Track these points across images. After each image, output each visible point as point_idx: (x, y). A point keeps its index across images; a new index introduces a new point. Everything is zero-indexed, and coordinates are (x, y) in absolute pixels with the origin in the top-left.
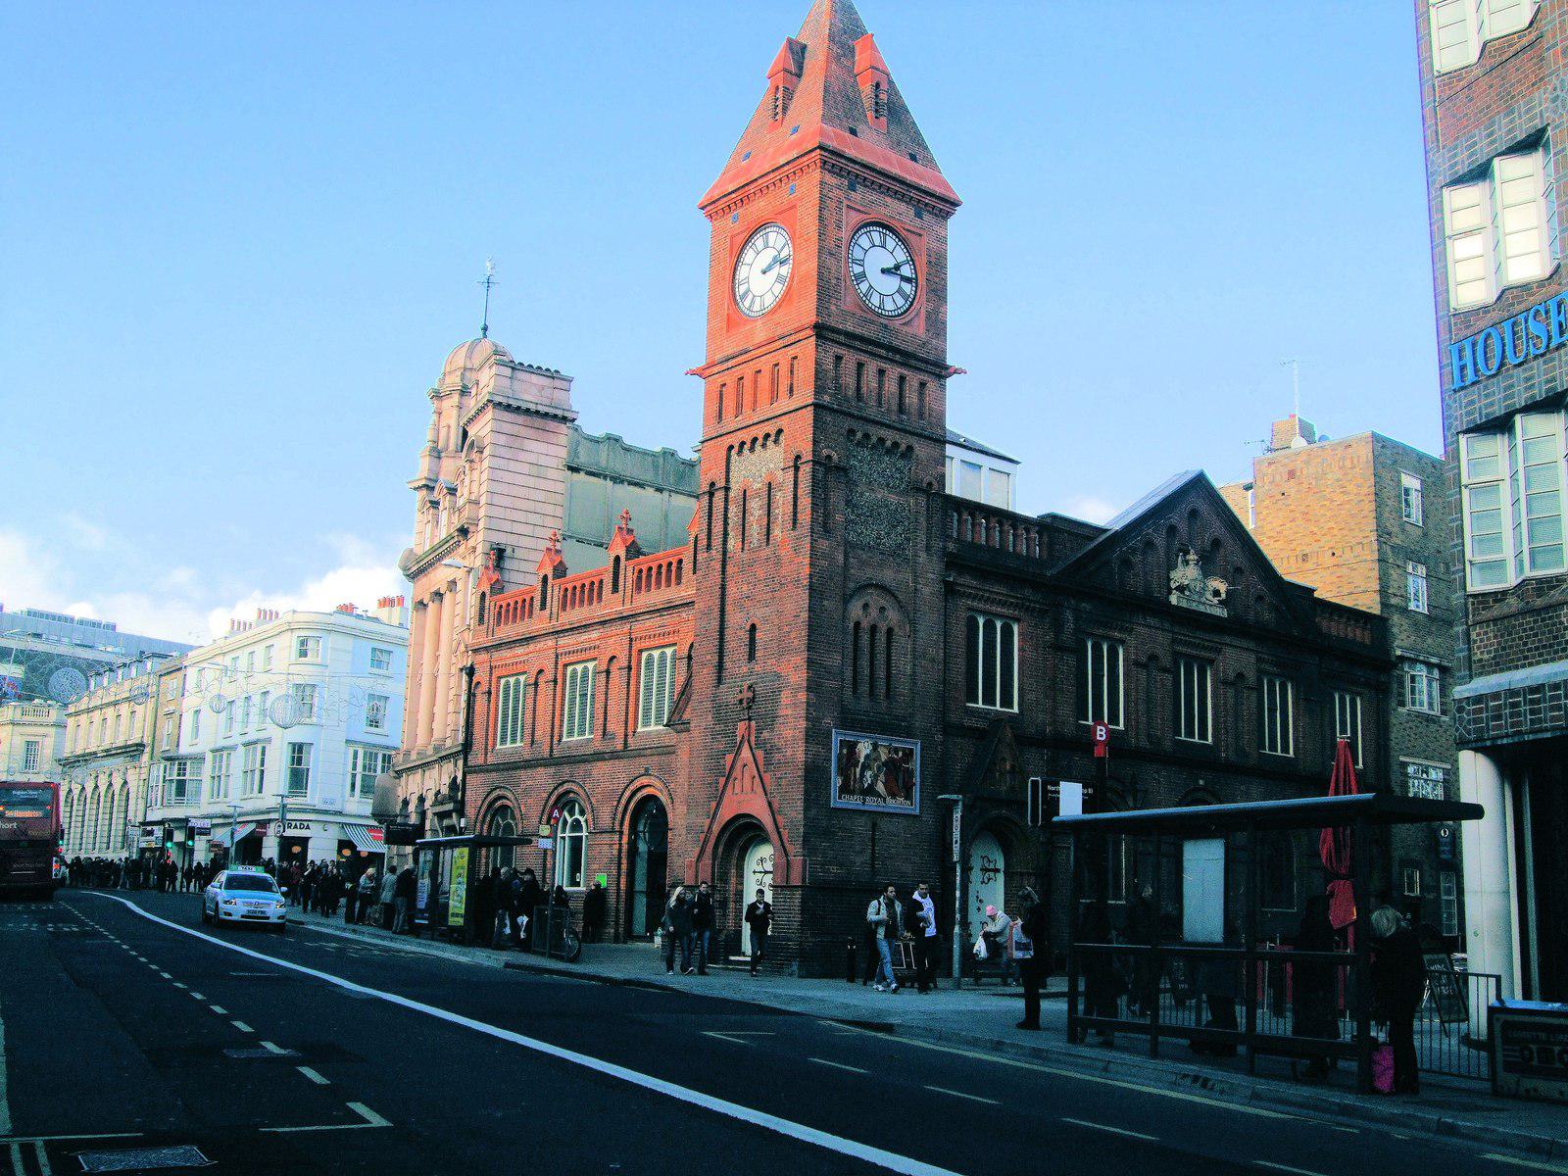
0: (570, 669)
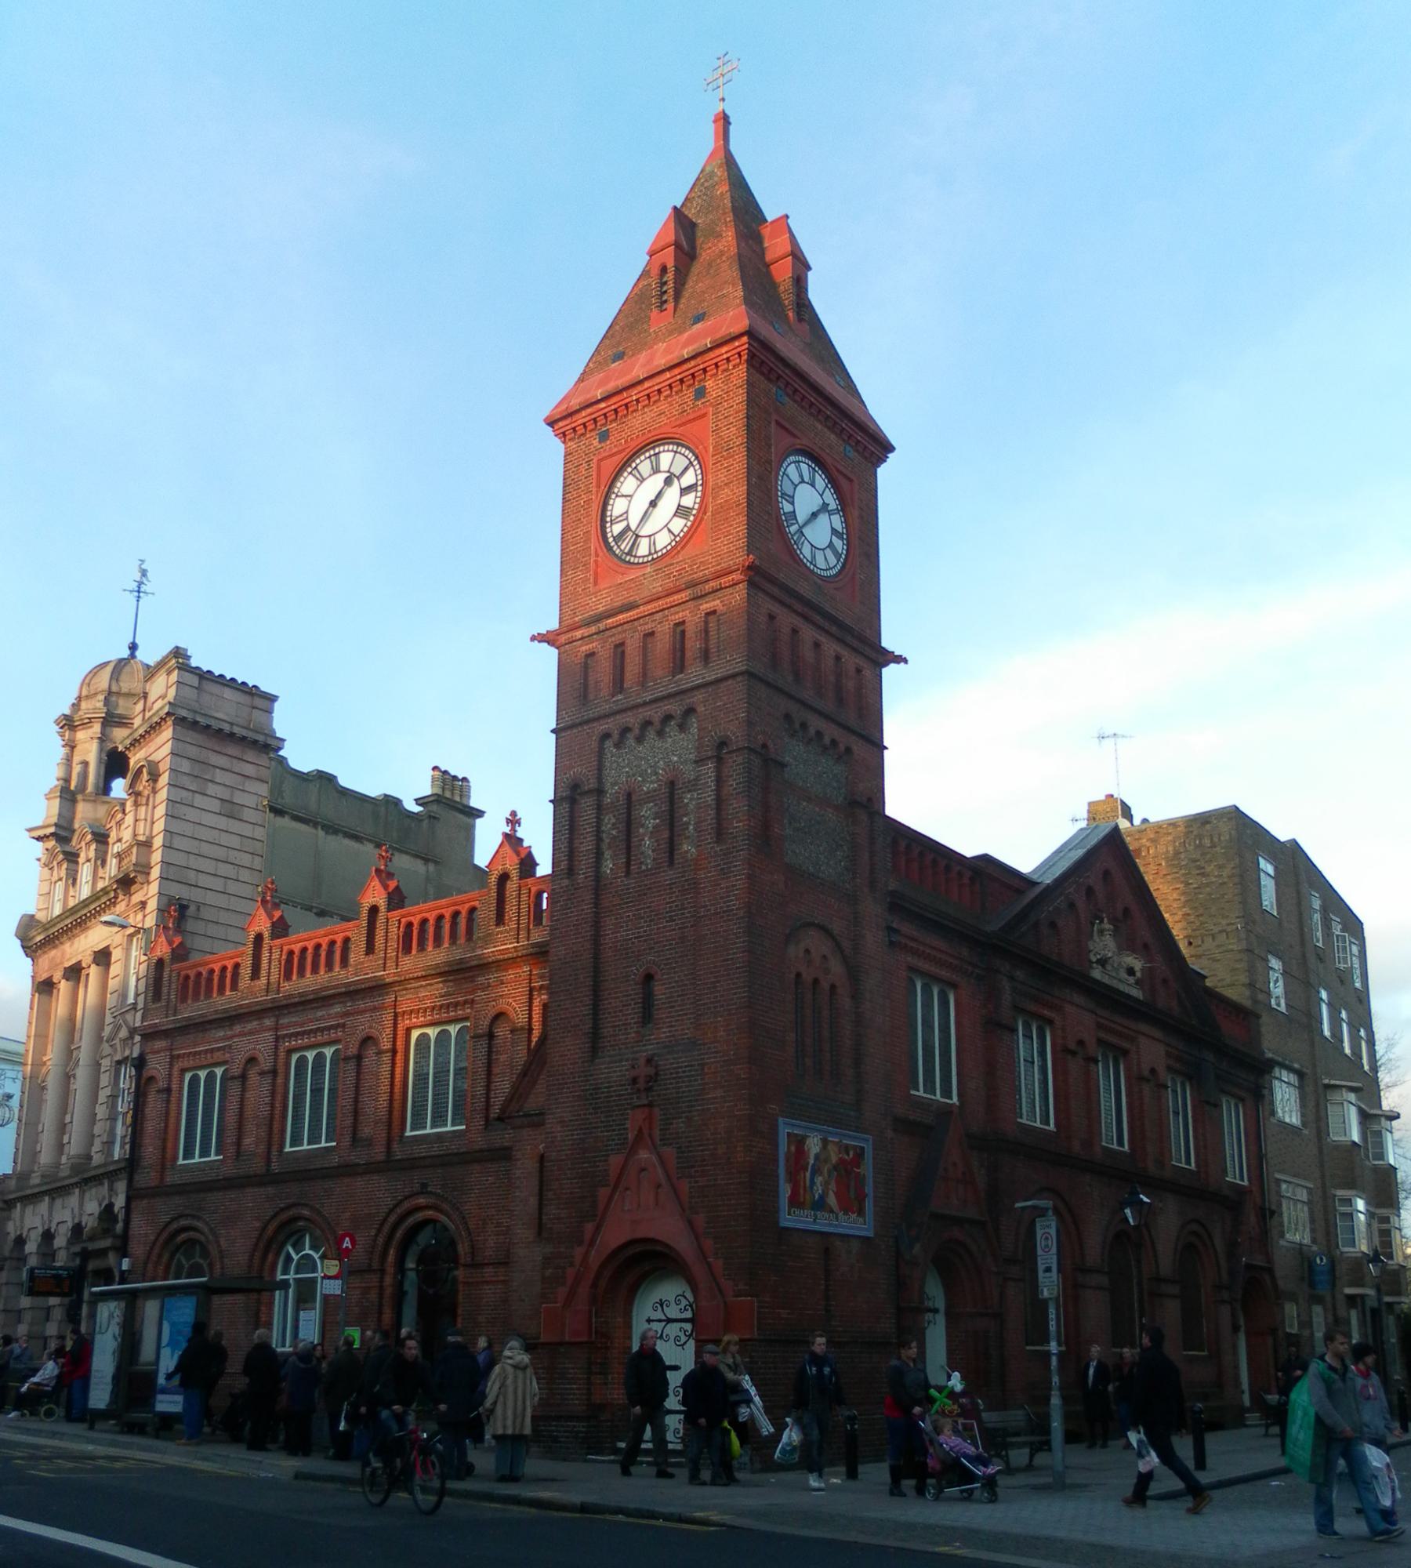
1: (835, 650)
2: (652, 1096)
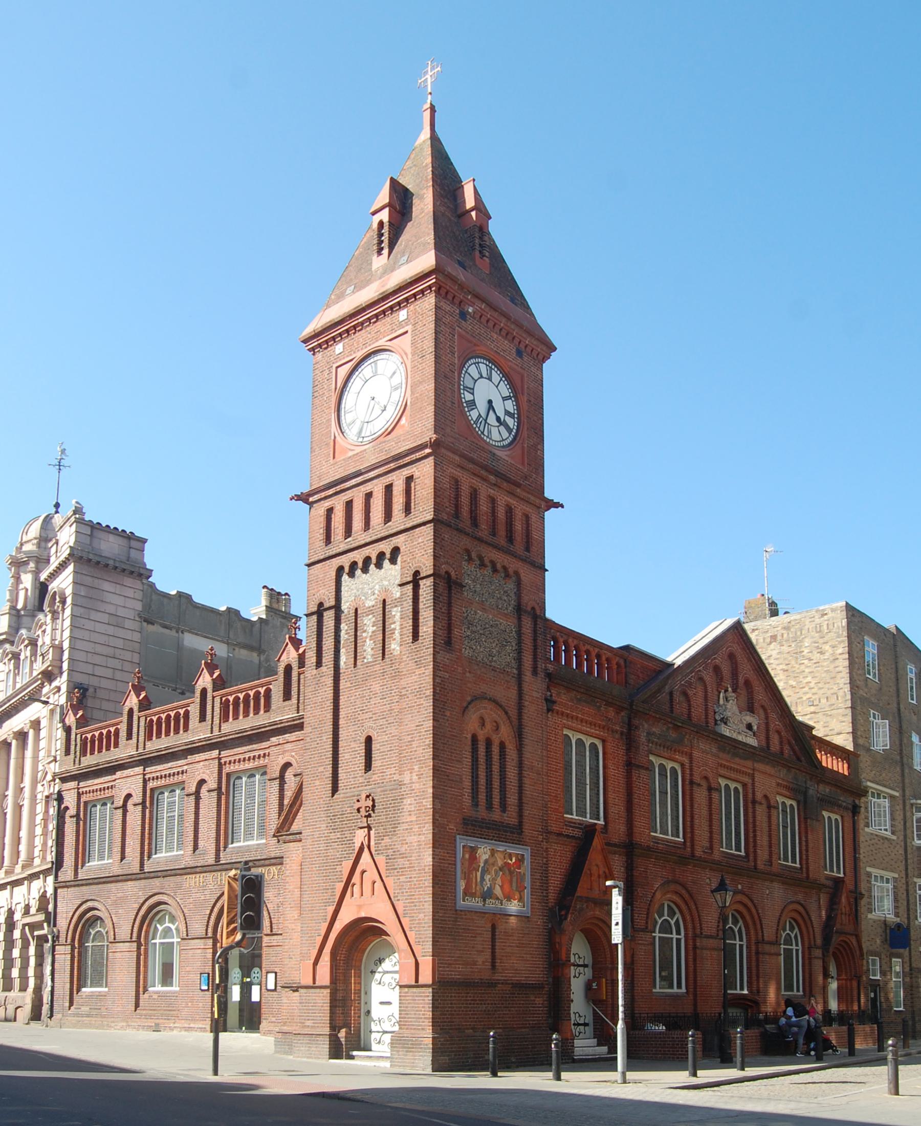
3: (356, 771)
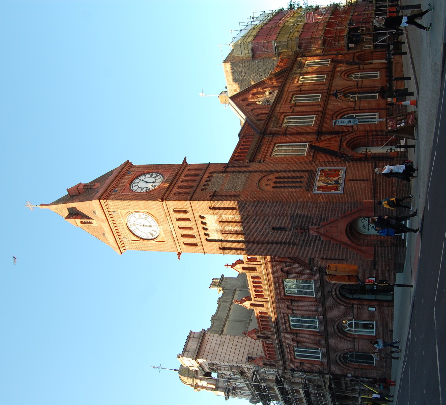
0: (292, 328)
1: (183, 177)
2: (306, 228)
3: (286, 234)
